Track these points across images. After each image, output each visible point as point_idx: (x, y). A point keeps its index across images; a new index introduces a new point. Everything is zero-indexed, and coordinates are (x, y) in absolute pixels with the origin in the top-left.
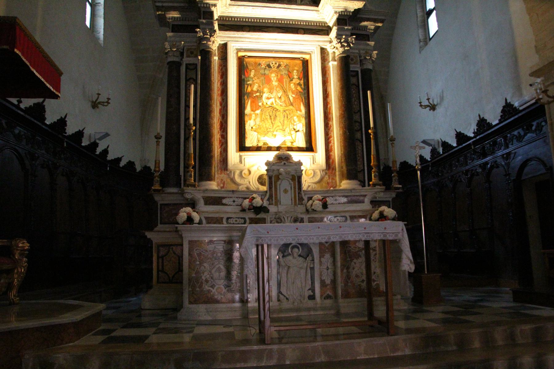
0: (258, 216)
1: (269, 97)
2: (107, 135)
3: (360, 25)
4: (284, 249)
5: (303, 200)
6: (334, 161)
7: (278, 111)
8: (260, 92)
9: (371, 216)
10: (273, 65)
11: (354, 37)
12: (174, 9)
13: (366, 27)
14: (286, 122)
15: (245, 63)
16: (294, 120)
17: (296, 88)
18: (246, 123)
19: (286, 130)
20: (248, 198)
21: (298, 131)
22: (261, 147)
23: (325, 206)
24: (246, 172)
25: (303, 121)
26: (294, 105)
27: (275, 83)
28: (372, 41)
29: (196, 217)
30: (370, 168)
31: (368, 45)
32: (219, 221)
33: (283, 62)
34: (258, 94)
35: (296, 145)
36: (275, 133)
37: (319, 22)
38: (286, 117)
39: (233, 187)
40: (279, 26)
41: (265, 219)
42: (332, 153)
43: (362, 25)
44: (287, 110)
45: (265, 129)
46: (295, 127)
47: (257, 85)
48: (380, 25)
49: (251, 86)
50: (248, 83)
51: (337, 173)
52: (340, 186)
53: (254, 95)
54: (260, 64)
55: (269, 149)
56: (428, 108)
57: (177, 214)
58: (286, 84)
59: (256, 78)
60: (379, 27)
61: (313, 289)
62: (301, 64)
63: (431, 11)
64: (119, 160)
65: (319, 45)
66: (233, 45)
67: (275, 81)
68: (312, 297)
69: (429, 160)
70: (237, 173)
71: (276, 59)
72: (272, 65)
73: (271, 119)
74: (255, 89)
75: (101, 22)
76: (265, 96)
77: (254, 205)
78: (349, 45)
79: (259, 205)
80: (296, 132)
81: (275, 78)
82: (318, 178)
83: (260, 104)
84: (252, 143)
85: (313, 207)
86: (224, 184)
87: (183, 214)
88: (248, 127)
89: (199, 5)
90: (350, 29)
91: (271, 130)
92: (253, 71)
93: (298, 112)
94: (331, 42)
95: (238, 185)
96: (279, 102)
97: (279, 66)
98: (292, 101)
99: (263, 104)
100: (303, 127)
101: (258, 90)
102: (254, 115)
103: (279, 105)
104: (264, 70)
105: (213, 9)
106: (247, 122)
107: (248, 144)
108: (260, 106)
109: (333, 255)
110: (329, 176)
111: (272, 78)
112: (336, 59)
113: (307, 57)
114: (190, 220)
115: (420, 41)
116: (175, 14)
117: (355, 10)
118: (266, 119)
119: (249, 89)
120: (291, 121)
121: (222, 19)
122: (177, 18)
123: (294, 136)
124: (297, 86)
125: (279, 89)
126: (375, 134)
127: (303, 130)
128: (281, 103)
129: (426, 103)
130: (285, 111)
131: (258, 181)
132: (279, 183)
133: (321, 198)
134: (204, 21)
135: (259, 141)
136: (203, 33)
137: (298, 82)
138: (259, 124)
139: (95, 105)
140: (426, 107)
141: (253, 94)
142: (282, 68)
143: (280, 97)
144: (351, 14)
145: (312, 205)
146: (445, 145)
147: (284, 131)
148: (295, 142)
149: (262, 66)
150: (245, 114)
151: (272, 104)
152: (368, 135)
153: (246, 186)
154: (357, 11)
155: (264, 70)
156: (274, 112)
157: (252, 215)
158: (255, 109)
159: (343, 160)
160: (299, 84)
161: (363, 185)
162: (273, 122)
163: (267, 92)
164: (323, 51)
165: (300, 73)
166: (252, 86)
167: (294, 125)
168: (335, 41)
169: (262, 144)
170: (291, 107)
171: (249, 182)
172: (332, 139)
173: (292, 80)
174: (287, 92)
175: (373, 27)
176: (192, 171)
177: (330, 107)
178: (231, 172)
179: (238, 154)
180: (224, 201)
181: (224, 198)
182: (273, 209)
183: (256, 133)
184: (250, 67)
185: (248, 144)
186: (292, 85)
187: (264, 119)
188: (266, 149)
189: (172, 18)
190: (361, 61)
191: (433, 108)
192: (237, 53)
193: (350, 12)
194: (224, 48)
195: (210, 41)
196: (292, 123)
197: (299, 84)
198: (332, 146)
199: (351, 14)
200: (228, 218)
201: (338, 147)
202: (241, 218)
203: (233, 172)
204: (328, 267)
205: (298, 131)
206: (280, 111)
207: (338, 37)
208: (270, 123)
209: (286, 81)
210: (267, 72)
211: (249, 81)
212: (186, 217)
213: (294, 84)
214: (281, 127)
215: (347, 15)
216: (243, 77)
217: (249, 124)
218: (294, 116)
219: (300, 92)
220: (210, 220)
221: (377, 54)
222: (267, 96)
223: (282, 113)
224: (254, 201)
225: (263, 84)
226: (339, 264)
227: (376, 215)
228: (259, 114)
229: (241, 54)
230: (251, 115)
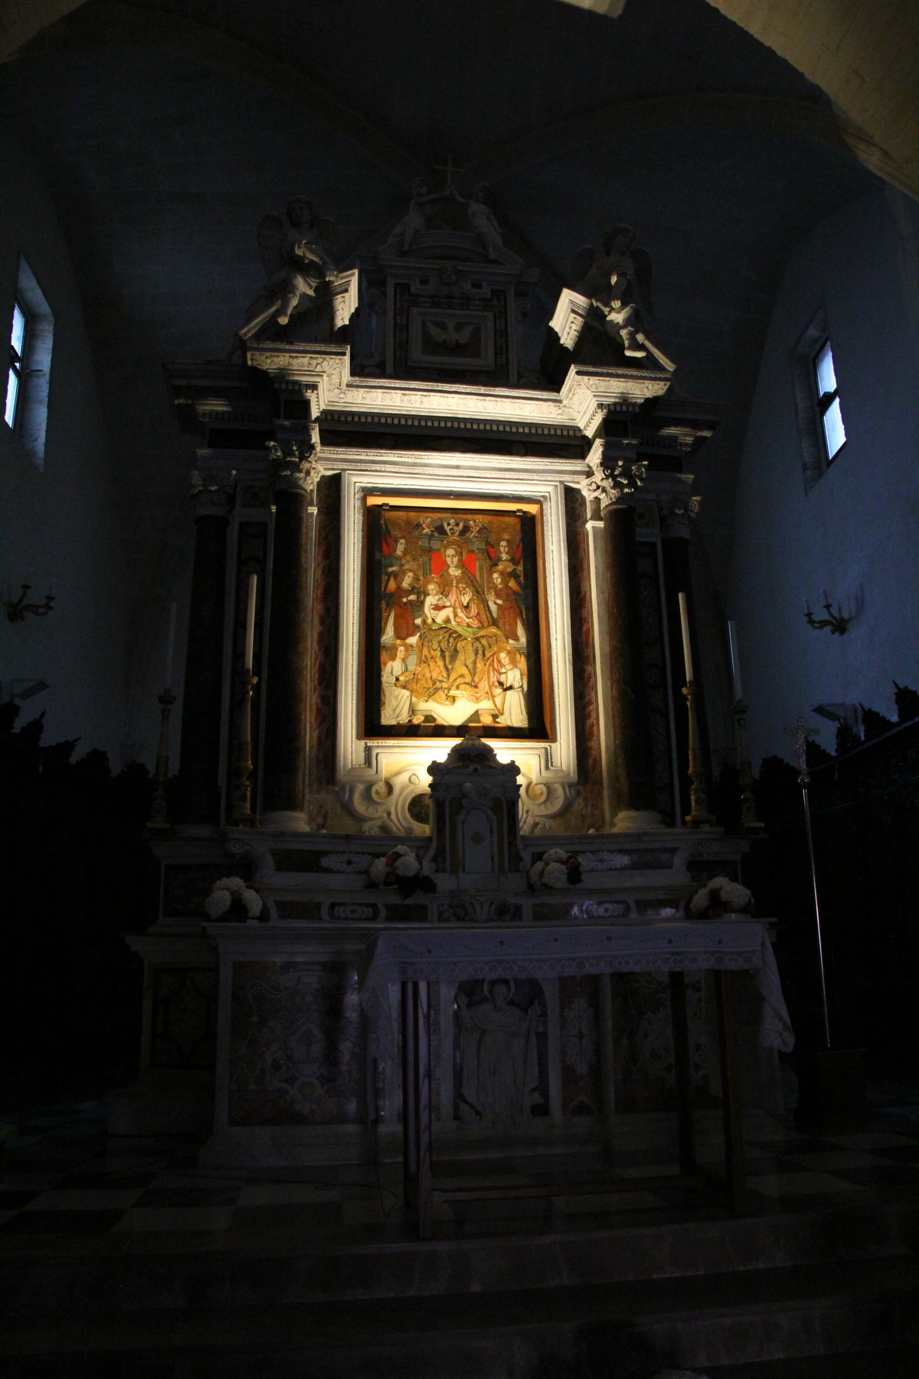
0: (407, 901)
1: (441, 603)
2: (42, 686)
3: (659, 434)
5: (520, 859)
6: (598, 761)
7: (463, 638)
8: (418, 594)
9: (690, 901)
10: (450, 527)
11: (646, 463)
12: (217, 393)
13: (674, 438)
14: (479, 665)
15: (382, 522)
16: (499, 662)
17: (505, 582)
18: (383, 667)
19: (479, 686)
20: (384, 855)
21: (511, 688)
22: (418, 726)
23: (575, 875)
24: (380, 787)
25: (523, 663)
26: (501, 625)
27: (454, 572)
28: (688, 473)
29: (253, 900)
30: (686, 782)
31: (679, 480)
32: (309, 911)
33: (475, 521)
34: (412, 597)
35: (503, 721)
36: (453, 692)
37: (563, 427)
38: (480, 652)
39: (347, 826)
40: (468, 435)
41: (425, 907)
42: (593, 744)
43: (665, 434)
44: (483, 637)
45: (430, 683)
46: (503, 678)
47: (411, 574)
48: (706, 434)
49: (395, 579)
50: (390, 569)
51: (606, 793)
52: (613, 825)
53: (405, 600)
54: (419, 526)
55: (440, 731)
56: (828, 629)
57: (206, 892)
58: (481, 573)
59: (408, 558)
60: (705, 438)
61: (543, 1089)
62: (518, 527)
63: (828, 399)
64: (68, 747)
65: (561, 482)
66: (354, 479)
67: (455, 567)
68: (541, 1110)
69: (834, 754)
70: (360, 788)
71: (456, 514)
72: (447, 528)
73: (443, 657)
74: (406, 584)
75: (41, 414)
76: (430, 601)
77: (400, 872)
78: (632, 484)
79: (411, 873)
80: (506, 690)
81: (456, 560)
82: (558, 804)
83: (418, 621)
84: (398, 716)
85: (545, 880)
86: (325, 817)
88: (387, 678)
89: (277, 386)
90: (635, 445)
91: (444, 685)
92: (402, 541)
93: (511, 641)
94: (589, 474)
95: (360, 819)
96: (465, 618)
97: (466, 529)
98: (495, 615)
99: (424, 622)
100: (522, 678)
101: (413, 588)
102: (402, 648)
103: (464, 622)
104: (430, 540)
105: (310, 395)
106: (385, 664)
107: (388, 718)
108: (417, 627)
109: (595, 1002)
110: (585, 799)
111: (448, 560)
112: (602, 514)
113: (532, 509)
114: (238, 909)
115: (805, 467)
116: (218, 406)
117: (647, 400)
118: (432, 658)
119: (392, 585)
120: (492, 665)
121: (329, 417)
122: (223, 413)
124: (508, 579)
125: (464, 586)
126: (699, 697)
127: (522, 687)
128: (468, 620)
129: (821, 615)
130: (477, 639)
131: (409, 809)
132: (461, 817)
133: (563, 855)
134: (286, 423)
135: (413, 711)
136: (283, 452)
137: (509, 570)
138: (415, 670)
139: (15, 613)
140: (823, 624)
141: (401, 597)
142: (471, 535)
143: (465, 604)
144: (637, 410)
145: (542, 874)
146: (871, 718)
147: (476, 687)
148: (502, 714)
149: (424, 529)
150: (382, 645)
151: (448, 621)
152: (680, 700)
153: (379, 822)
154: (651, 403)
155: (430, 540)
156: (451, 640)
157: (395, 899)
158: (404, 633)
159: (620, 761)
160: (513, 575)
161: (669, 820)
162: (450, 667)
163: (434, 592)
164: (572, 497)
165: (515, 548)
166: (399, 578)
167: (500, 674)
168: (599, 476)
169: (422, 718)
170: (494, 630)
171: (389, 814)
172: (592, 707)
173: (496, 565)
174: (484, 593)
175: (689, 440)
176: (247, 786)
177: (588, 630)
178: (343, 788)
179: (363, 742)
180: (325, 862)
181: (326, 853)
182: (444, 882)
183: (406, 693)
184: (395, 533)
185: (388, 718)
186: (495, 575)
187: (427, 659)
188: (431, 730)
189: (211, 412)
190: (662, 519)
191: (840, 626)
192: (364, 500)
193: (635, 404)
195: (300, 471)
196: (494, 669)
197: (513, 575)
198: (592, 726)
199: (637, 410)
200: (333, 906)
201: (606, 727)
202: (368, 905)
203: (348, 787)
204: (580, 1032)
205: (511, 688)
206: (465, 639)
207: (607, 463)
208: (442, 669)
209: (481, 568)
210: (435, 545)
211: (392, 566)
212: (229, 902)
213: (502, 573)
214: (468, 679)
215: (627, 412)
216: (378, 555)
217: (392, 669)
218: (500, 651)
219: (515, 593)
220: (288, 910)
221: (701, 503)
222: (435, 602)
223: (470, 645)
224: (399, 863)
225: (425, 574)
226: (609, 1025)
227: (700, 899)
228: (414, 645)
229: (373, 501)
230: (394, 648)
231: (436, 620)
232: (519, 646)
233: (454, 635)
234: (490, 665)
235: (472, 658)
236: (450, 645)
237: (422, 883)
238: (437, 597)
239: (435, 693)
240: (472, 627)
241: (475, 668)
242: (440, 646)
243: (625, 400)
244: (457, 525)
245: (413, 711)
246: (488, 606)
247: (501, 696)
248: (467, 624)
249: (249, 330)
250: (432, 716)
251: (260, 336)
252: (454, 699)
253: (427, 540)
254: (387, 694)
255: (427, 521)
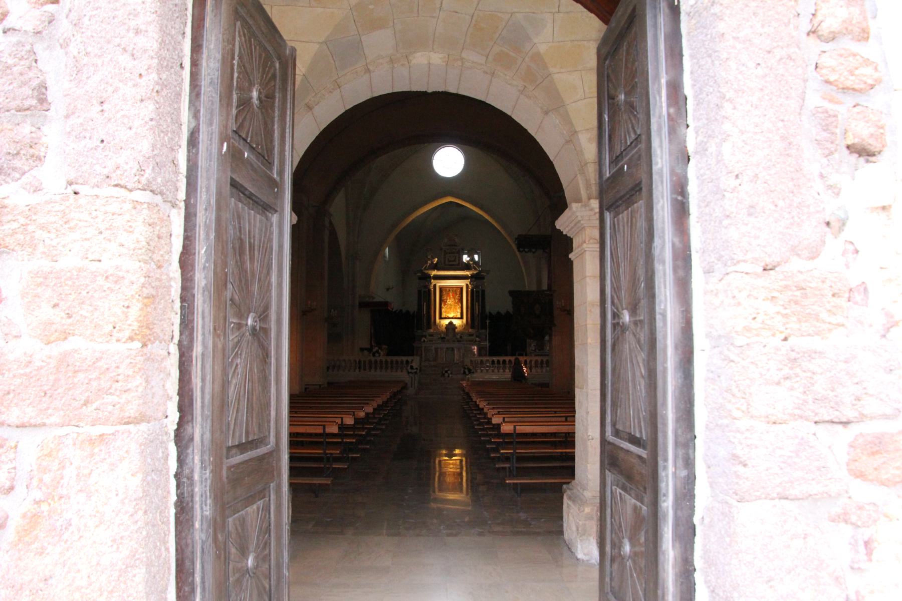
4: (447, 348)
29: (426, 340)
87: (422, 340)
107: (443, 316)
114: (424, 341)
139: (388, 289)
164: (467, 285)
182: (447, 338)
185: (443, 316)
194: (435, 286)
217: (443, 310)
220: (430, 341)
237: (444, 338)
243: (473, 273)
249: (423, 269)
251: (425, 269)
255: (448, 289)
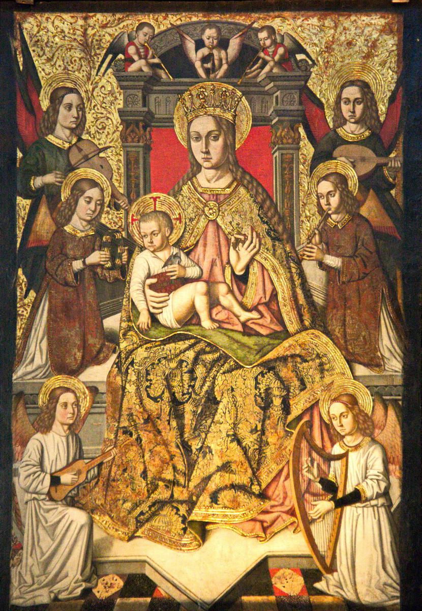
1: (174, 270)
10: (204, 51)
18: (17, 448)
19: (270, 493)
21: (355, 497)
38: (277, 402)
44: (284, 359)
46: (335, 470)
50: (37, 182)
53: (77, 265)
96: (237, 309)
98: (319, 299)
100: (387, 472)
120: (306, 435)
123: (321, 533)
127: (386, 494)
128: (244, 316)
138: (104, 454)
148: (331, 569)
150: (16, 389)
151: (191, 317)
155: (146, 92)
167: (329, 459)
183: (78, 517)
196: (312, 447)
205: (355, 497)
211: (44, 173)
219: (377, 234)
222: (157, 267)
228: (102, 388)
231: (160, 317)
232: (382, 383)
233: (209, 357)
234: (302, 434)
235: (254, 421)
236: (198, 384)
238: (164, 255)
239: (154, 515)
240: (258, 334)
241: (262, 444)
242: (169, 387)
244: (223, 44)
245: (94, 564)
246: (302, 274)
247: (329, 519)
248: (244, 325)
250: (145, 578)
252: (203, 530)
253: (140, 94)
254: (27, 521)
